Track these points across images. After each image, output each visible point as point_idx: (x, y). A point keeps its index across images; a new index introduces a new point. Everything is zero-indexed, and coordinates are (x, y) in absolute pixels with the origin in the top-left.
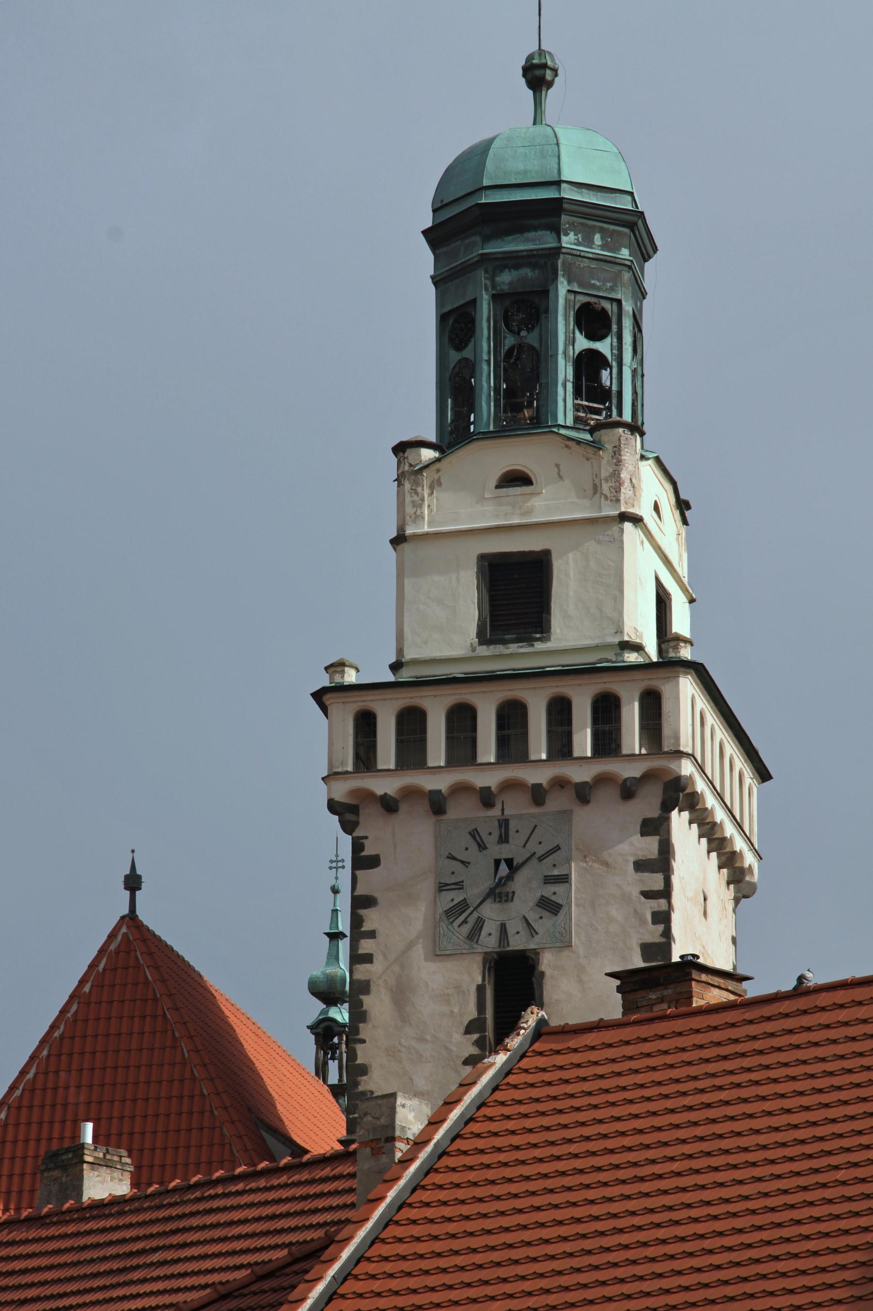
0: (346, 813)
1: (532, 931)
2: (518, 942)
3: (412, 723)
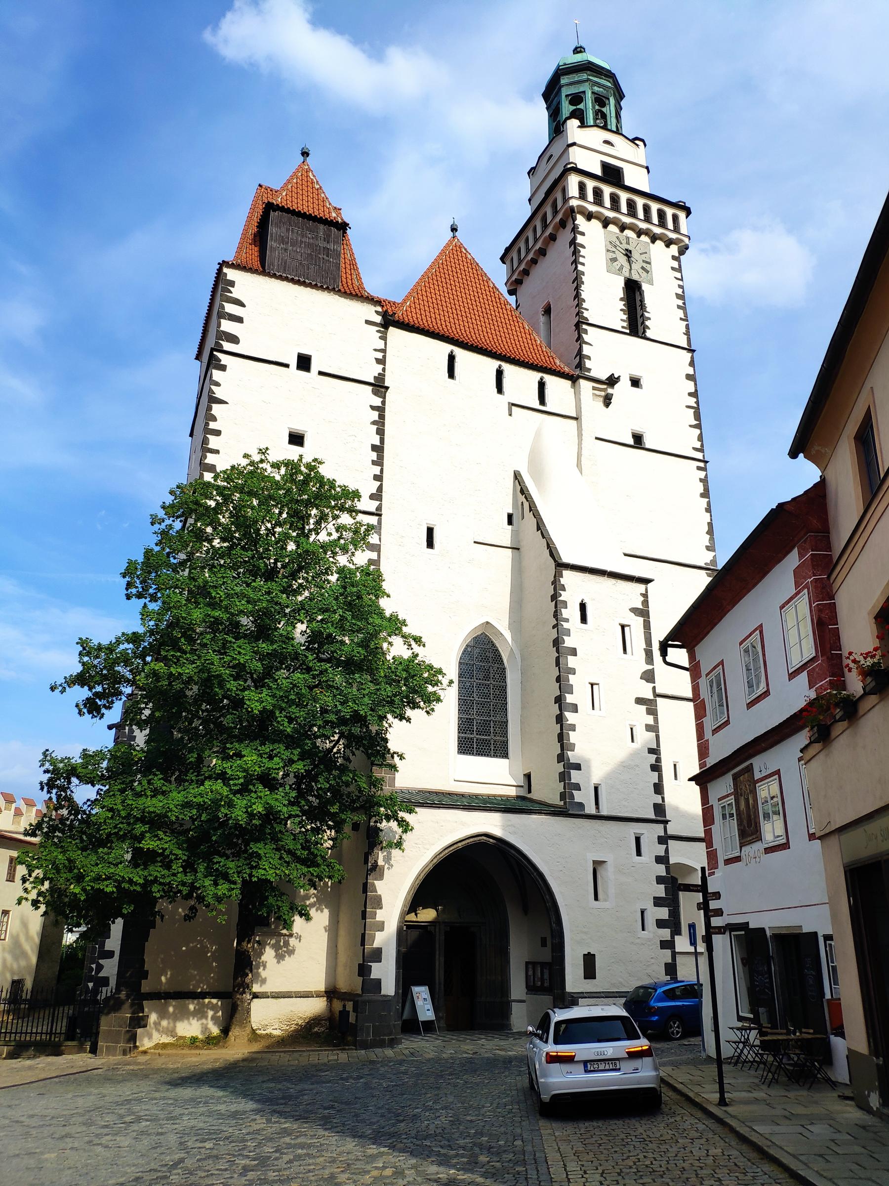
1: (640, 276)
2: (635, 277)
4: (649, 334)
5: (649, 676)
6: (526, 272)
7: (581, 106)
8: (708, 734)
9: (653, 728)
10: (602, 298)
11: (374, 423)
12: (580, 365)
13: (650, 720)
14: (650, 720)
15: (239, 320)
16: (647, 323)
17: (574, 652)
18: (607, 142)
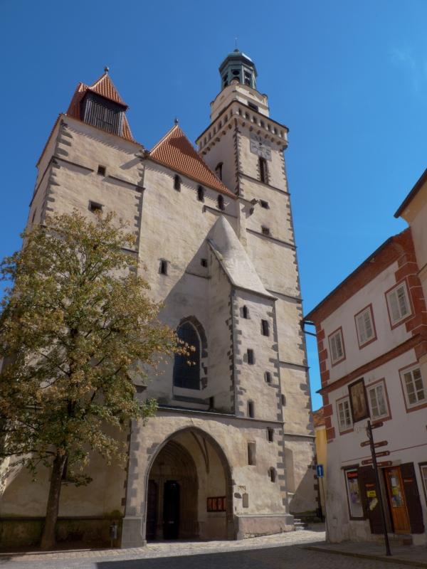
2: (264, 156)
4: (270, 183)
5: (275, 348)
6: (209, 149)
7: (238, 76)
8: (328, 367)
9: (277, 375)
10: (249, 165)
11: (137, 205)
12: (238, 193)
13: (276, 370)
14: (276, 370)
15: (69, 144)
16: (269, 178)
17: (240, 332)
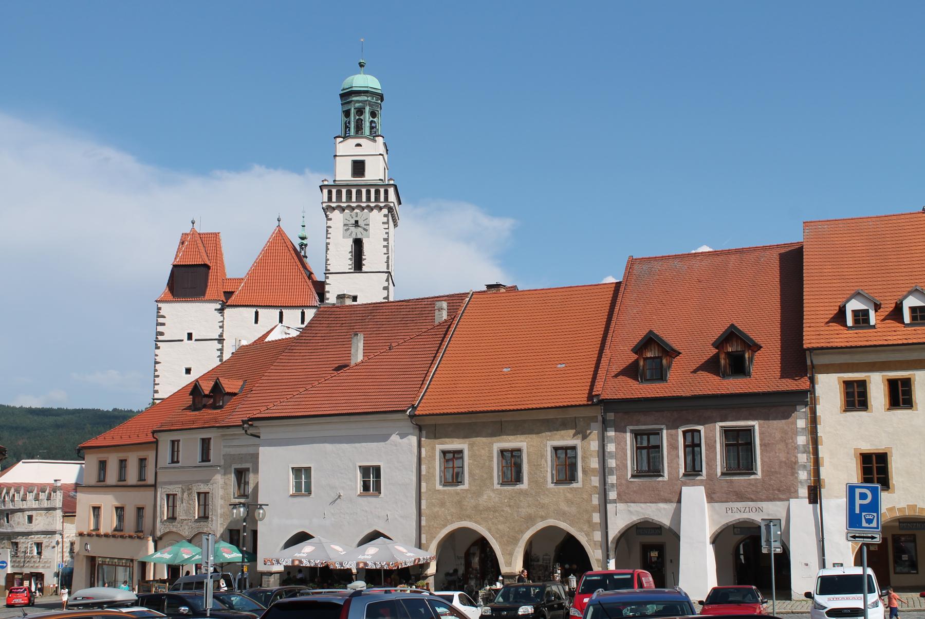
0: (325, 210)
2: (359, 237)
3: (339, 193)
15: (163, 324)
18: (358, 145)
